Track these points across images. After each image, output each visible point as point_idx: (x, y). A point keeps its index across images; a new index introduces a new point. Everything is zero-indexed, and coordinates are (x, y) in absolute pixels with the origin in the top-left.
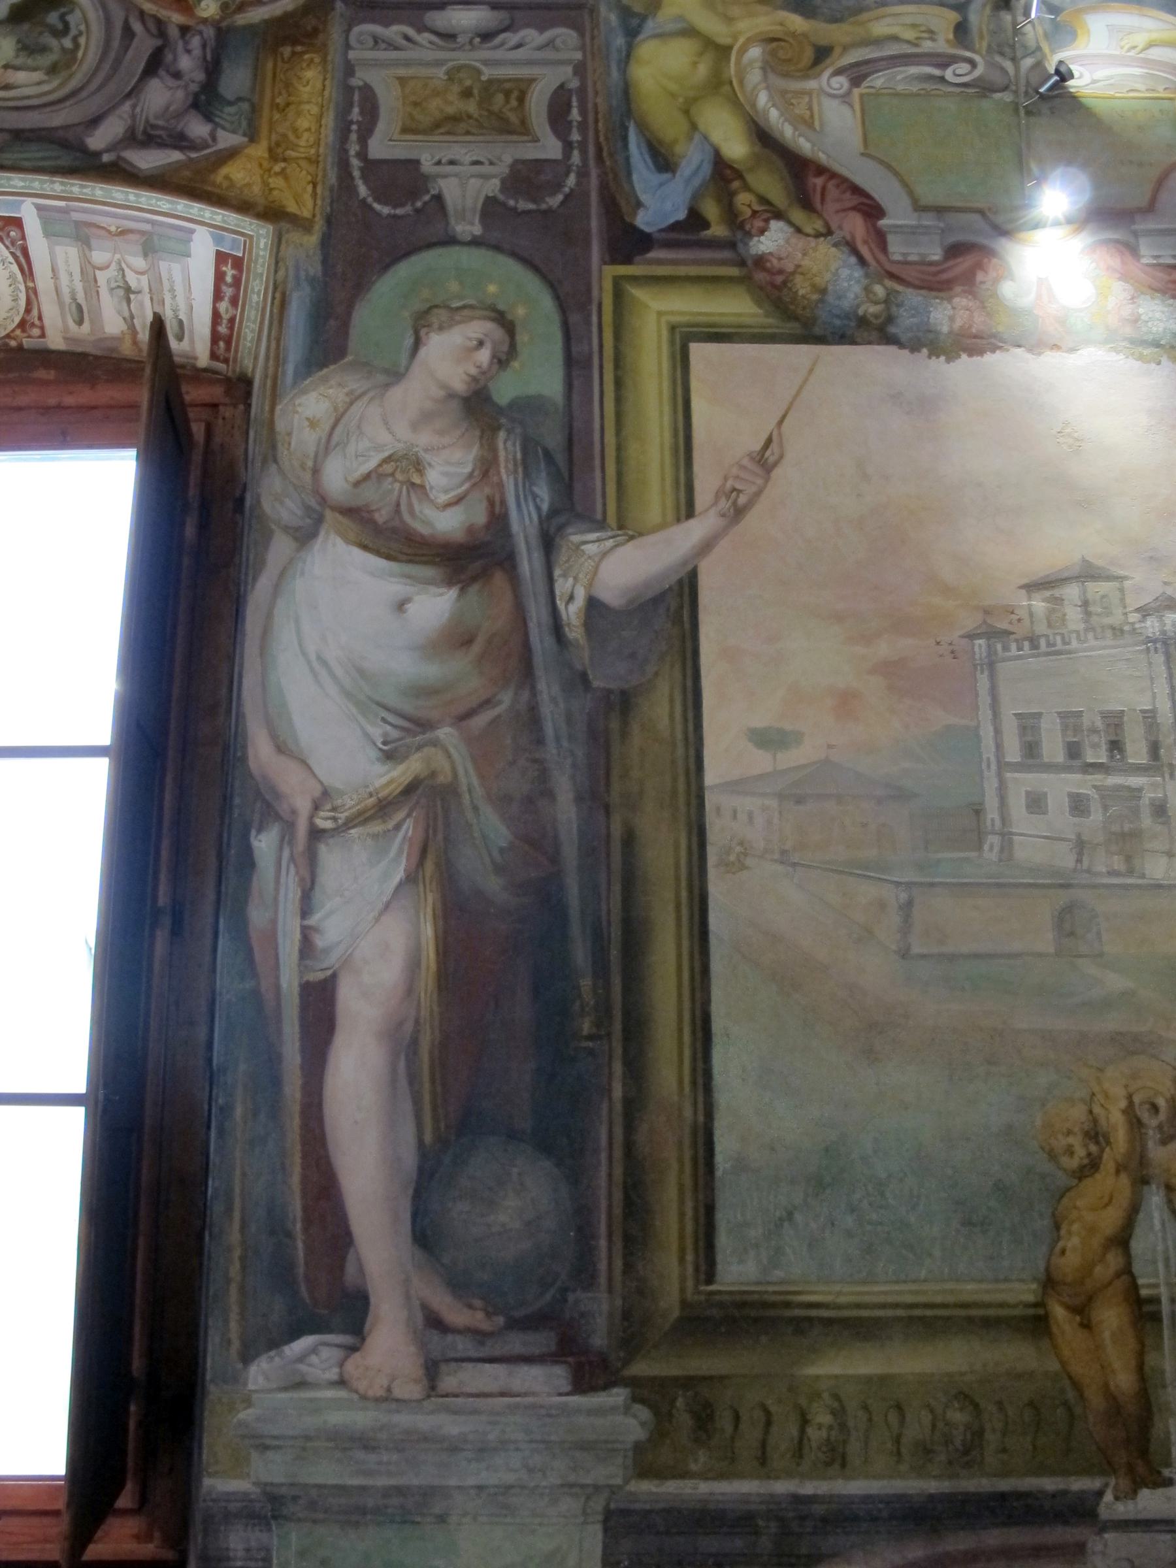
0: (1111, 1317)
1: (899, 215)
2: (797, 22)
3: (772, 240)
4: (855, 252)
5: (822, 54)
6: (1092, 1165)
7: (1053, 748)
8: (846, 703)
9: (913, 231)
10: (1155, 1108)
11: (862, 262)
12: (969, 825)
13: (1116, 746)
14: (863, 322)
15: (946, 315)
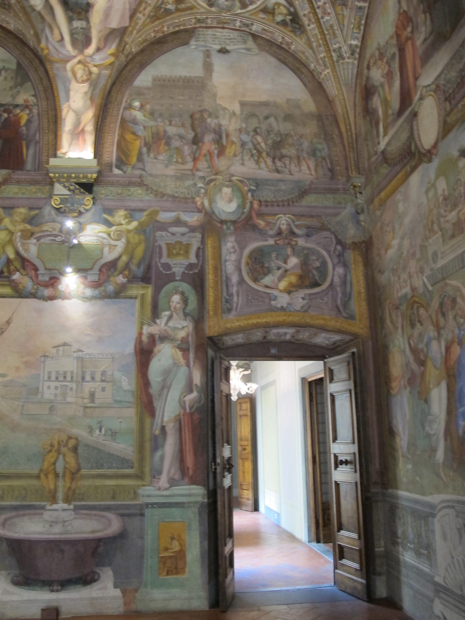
0: (51, 476)
1: (42, 271)
2: (28, 227)
3: (16, 276)
4: (32, 279)
5: (32, 234)
6: (50, 451)
7: (53, 378)
8: (17, 369)
9: (43, 274)
10: (63, 441)
11: (33, 281)
12: (36, 391)
13: (65, 377)
14: (31, 294)
15: (47, 292)
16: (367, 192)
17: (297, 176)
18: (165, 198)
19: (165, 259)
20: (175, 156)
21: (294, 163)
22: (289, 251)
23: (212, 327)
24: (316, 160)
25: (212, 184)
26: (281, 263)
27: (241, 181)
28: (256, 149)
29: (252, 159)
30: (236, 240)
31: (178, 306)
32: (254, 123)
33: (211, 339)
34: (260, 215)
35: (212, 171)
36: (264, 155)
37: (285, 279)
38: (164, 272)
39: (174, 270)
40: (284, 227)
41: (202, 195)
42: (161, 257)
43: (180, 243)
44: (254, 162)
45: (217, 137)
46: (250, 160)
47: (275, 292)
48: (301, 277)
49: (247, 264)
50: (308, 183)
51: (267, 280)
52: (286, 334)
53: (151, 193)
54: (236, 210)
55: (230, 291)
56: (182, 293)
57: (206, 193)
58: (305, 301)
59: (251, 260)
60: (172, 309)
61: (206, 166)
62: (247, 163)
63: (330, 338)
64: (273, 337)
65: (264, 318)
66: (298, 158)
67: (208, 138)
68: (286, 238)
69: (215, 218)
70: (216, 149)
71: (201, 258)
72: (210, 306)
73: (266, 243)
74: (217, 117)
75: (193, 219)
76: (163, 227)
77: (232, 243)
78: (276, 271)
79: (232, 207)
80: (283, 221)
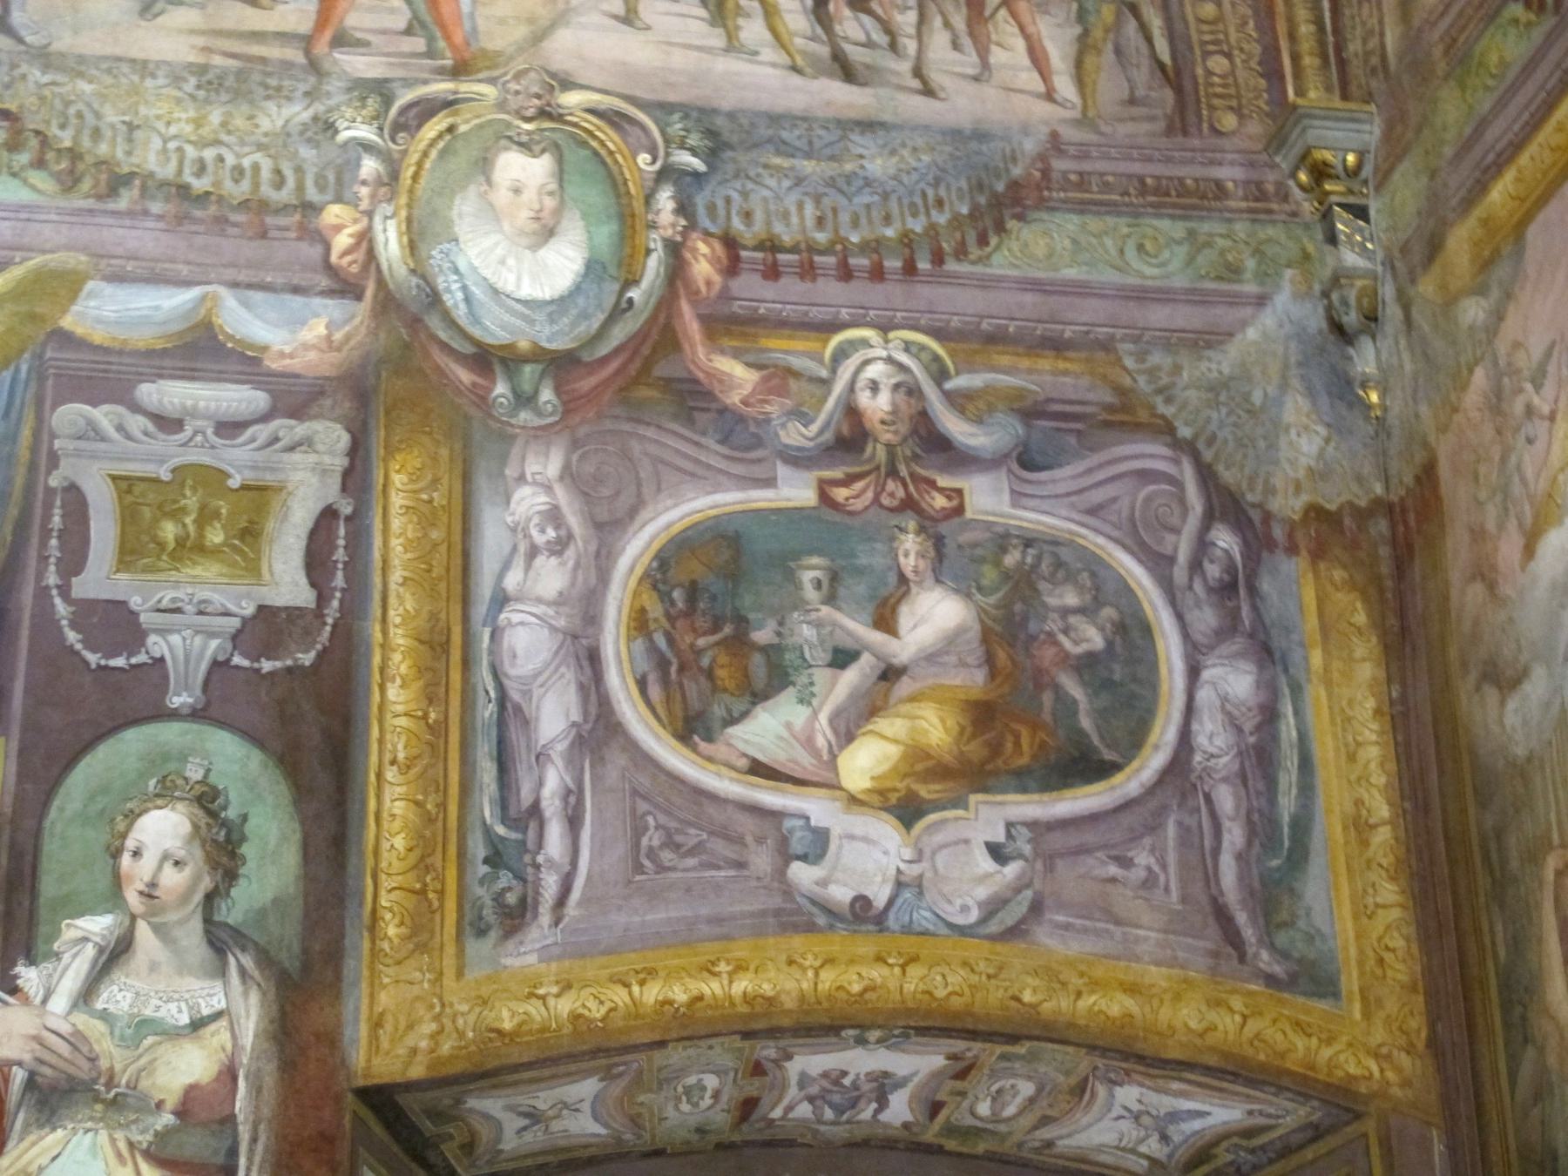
16: (1400, 200)
17: (963, 104)
18: (123, 202)
19: (100, 578)
21: (947, 24)
22: (910, 548)
24: (1082, 16)
25: (431, 129)
26: (858, 628)
27: (614, 119)
30: (568, 474)
31: (172, 879)
33: (381, 1100)
34: (728, 325)
35: (431, 53)
37: (882, 724)
38: (93, 658)
39: (157, 645)
40: (876, 406)
41: (364, 191)
42: (74, 562)
43: (210, 478)
44: (703, 13)
47: (817, 808)
48: (982, 715)
49: (640, 623)
50: (1030, 146)
51: (768, 729)
52: (883, 1086)
53: (40, 163)
54: (577, 290)
55: (526, 797)
56: (207, 800)
58: (1012, 870)
59: (666, 597)
60: (133, 899)
61: (401, 24)
63: (1174, 1117)
64: (804, 1110)
65: (740, 968)
68: (893, 472)
69: (443, 335)
71: (339, 580)
72: (386, 883)
73: (761, 498)
75: (302, 333)
76: (106, 374)
77: (548, 488)
78: (821, 676)
79: (558, 267)
80: (874, 370)
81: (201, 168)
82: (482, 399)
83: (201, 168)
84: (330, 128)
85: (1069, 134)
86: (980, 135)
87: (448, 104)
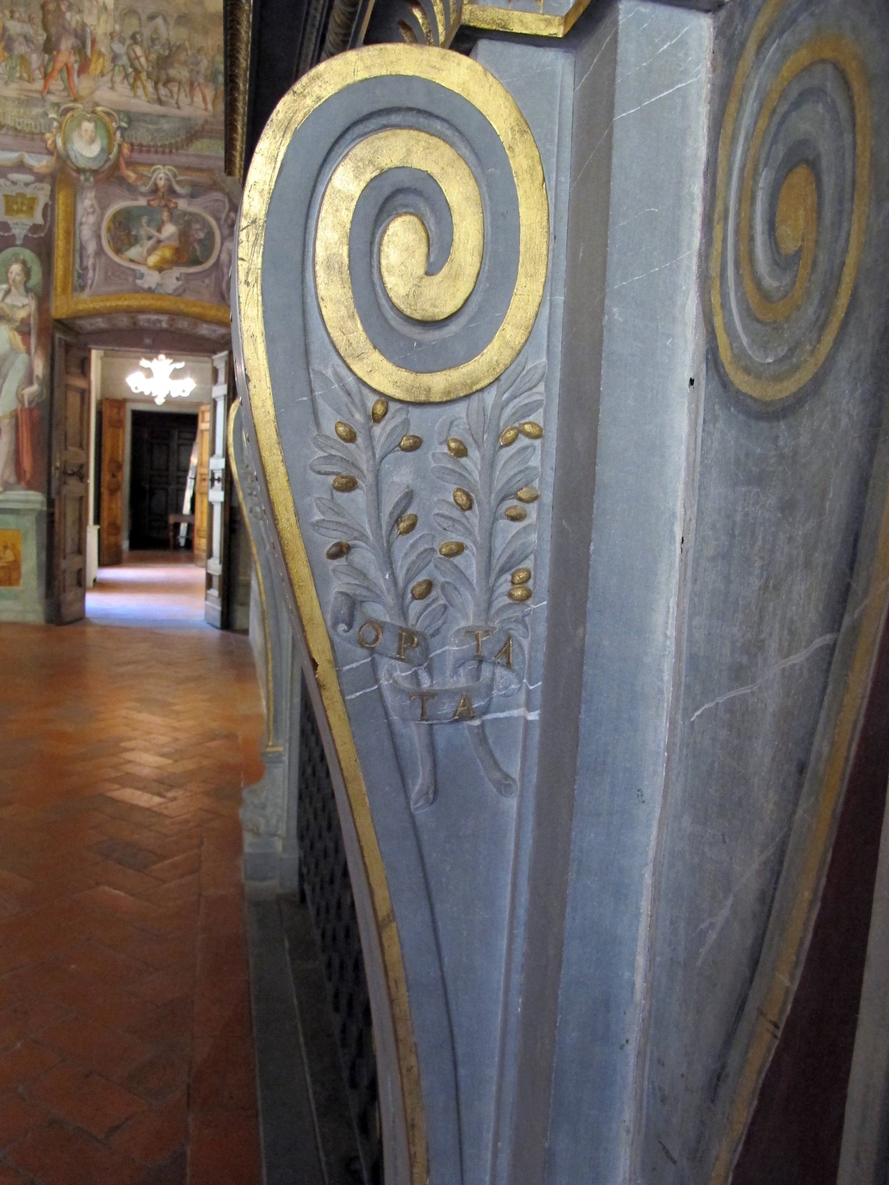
17: (186, 111)
20: (18, 68)
22: (165, 215)
23: (60, 307)
24: (216, 89)
25: (69, 115)
26: (153, 232)
28: (132, 66)
29: (126, 82)
30: (96, 197)
32: (132, 26)
33: (59, 321)
34: (130, 164)
35: (69, 96)
36: (144, 76)
40: (161, 183)
43: (23, 195)
45: (79, 42)
46: (122, 83)
48: (177, 251)
49: (109, 230)
50: (200, 122)
51: (134, 252)
54: (99, 155)
55: (85, 263)
56: (24, 263)
57: (60, 127)
58: (180, 283)
60: (10, 281)
61: (62, 87)
62: (118, 86)
65: (125, 300)
66: (192, 84)
67: (66, 44)
68: (163, 198)
70: (76, 61)
73: (135, 203)
74: (80, 11)
75: (41, 163)
77: (91, 200)
78: (145, 241)
80: (161, 175)
81: (19, 124)
82: (78, 180)
83: (19, 124)
84: (47, 115)
85: (210, 119)
86: (189, 119)
87: (72, 109)
